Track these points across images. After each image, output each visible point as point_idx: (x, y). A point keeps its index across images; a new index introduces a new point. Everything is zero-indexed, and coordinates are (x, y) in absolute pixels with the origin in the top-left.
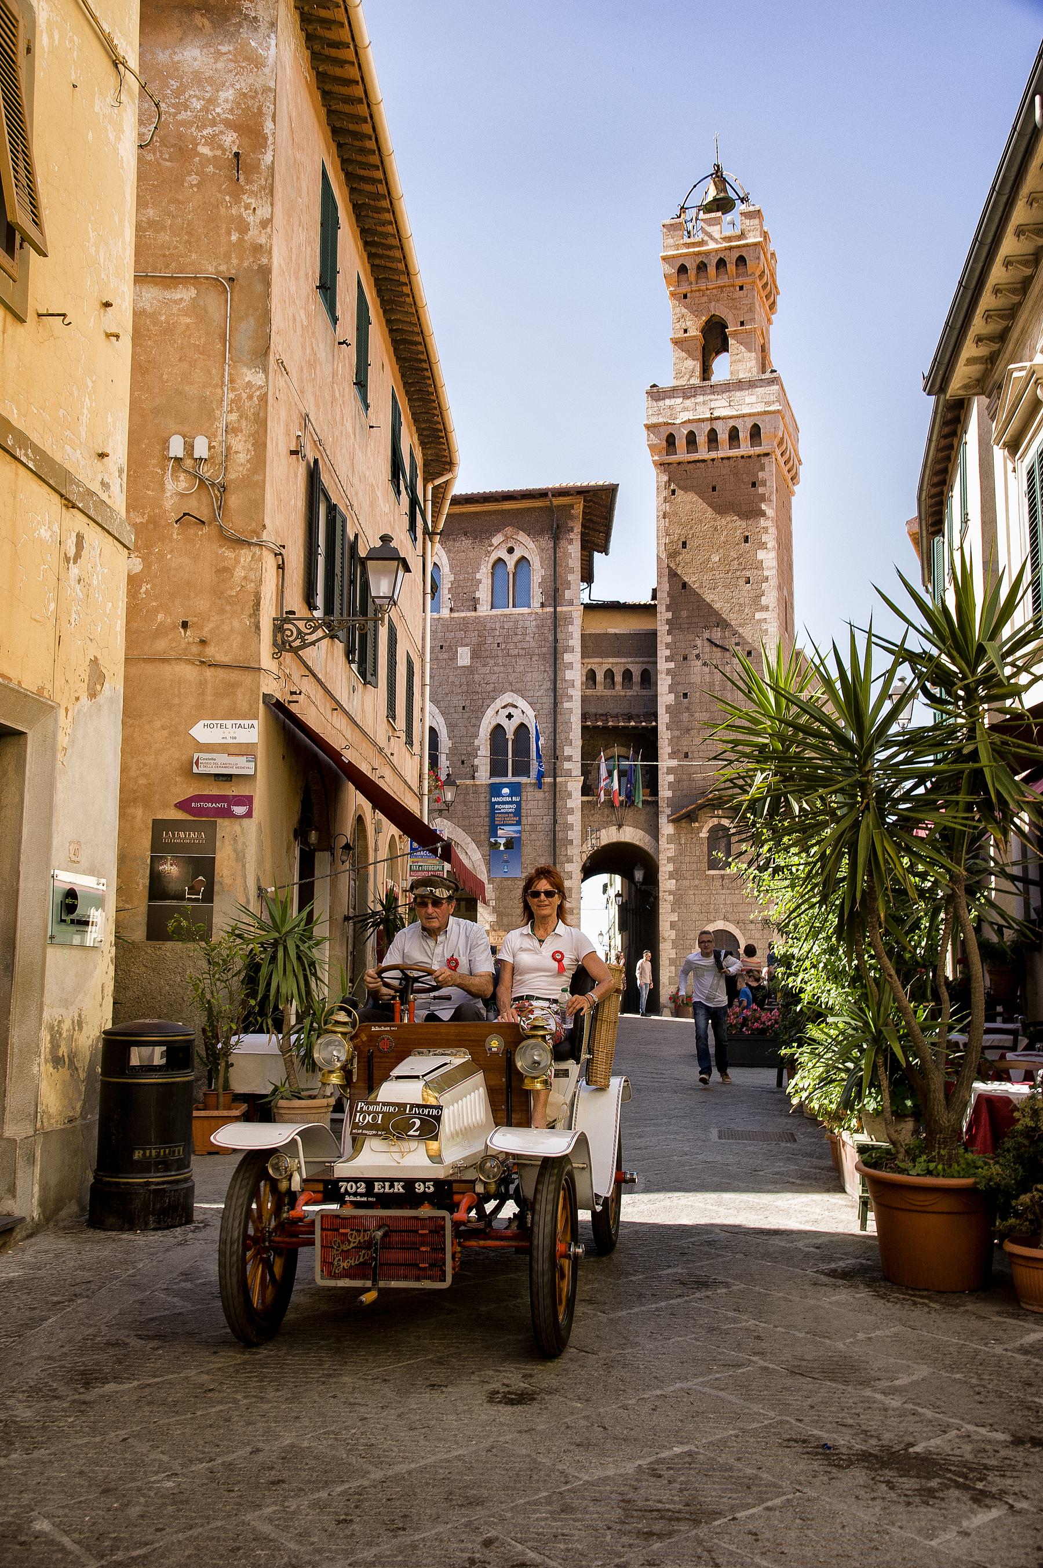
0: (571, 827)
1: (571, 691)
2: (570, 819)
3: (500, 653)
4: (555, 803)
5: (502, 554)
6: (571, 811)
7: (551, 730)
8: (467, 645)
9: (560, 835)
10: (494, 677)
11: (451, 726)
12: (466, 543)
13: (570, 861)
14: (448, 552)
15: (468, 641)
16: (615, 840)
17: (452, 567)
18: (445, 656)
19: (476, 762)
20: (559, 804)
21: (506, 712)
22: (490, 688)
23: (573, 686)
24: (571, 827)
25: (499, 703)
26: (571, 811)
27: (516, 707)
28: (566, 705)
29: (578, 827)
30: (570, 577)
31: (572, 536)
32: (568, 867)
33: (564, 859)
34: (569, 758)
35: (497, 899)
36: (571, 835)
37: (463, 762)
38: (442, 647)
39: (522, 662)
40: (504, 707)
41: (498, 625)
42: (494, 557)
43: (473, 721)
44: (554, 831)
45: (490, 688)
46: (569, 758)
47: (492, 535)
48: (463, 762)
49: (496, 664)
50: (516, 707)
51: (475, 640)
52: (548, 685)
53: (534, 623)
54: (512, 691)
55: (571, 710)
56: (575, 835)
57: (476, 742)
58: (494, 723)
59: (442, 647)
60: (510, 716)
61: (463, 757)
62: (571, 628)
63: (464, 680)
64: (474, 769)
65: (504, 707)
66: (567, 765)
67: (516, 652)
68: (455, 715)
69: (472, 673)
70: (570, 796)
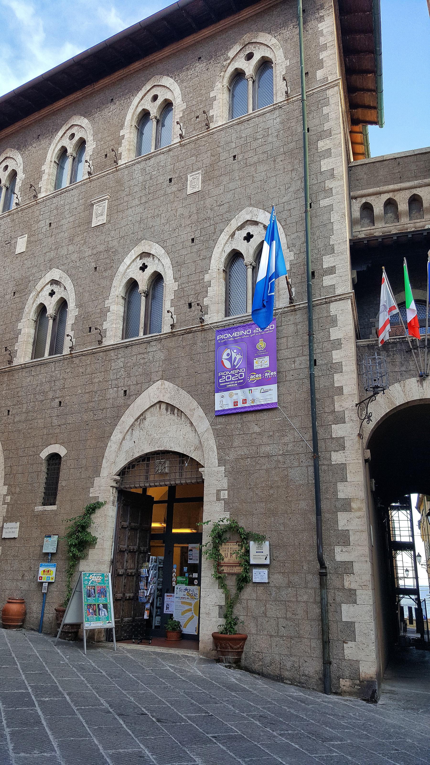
0: (338, 368)
1: (329, 184)
2: (337, 356)
3: (236, 166)
4: (310, 334)
5: (241, 63)
6: (337, 344)
7: (303, 239)
8: (199, 169)
9: (321, 383)
10: (229, 196)
11: (177, 265)
12: (200, 66)
13: (340, 419)
14: (181, 82)
15: (200, 164)
16: (416, 397)
17: (184, 96)
18: (174, 188)
19: (206, 301)
20: (318, 336)
21: (244, 233)
22: (223, 209)
23: (332, 176)
24: (338, 368)
25: (235, 223)
26: (337, 344)
27: (256, 223)
28: (324, 203)
29: (350, 367)
30: (323, 55)
31: (322, 13)
32: (337, 430)
33: (331, 418)
34: (332, 270)
35: (231, 488)
36: (339, 380)
37: (190, 305)
38: (170, 180)
39: (261, 168)
40: (240, 228)
41: (234, 136)
42: (231, 69)
43: (204, 253)
44: (312, 377)
45: (223, 209)
46: (332, 270)
47: (228, 49)
48: (190, 305)
49: (232, 180)
50: (256, 223)
51: (207, 161)
52: (299, 184)
53: (278, 120)
54: (251, 205)
55: (330, 208)
56: (347, 380)
57: (207, 277)
58: (228, 250)
59: (170, 180)
60: (249, 237)
61: (191, 299)
62: (325, 110)
63: (194, 209)
64: (204, 310)
65: (240, 228)
66: (327, 281)
67: (255, 159)
68: (184, 252)
69: (203, 198)
70: (333, 321)
